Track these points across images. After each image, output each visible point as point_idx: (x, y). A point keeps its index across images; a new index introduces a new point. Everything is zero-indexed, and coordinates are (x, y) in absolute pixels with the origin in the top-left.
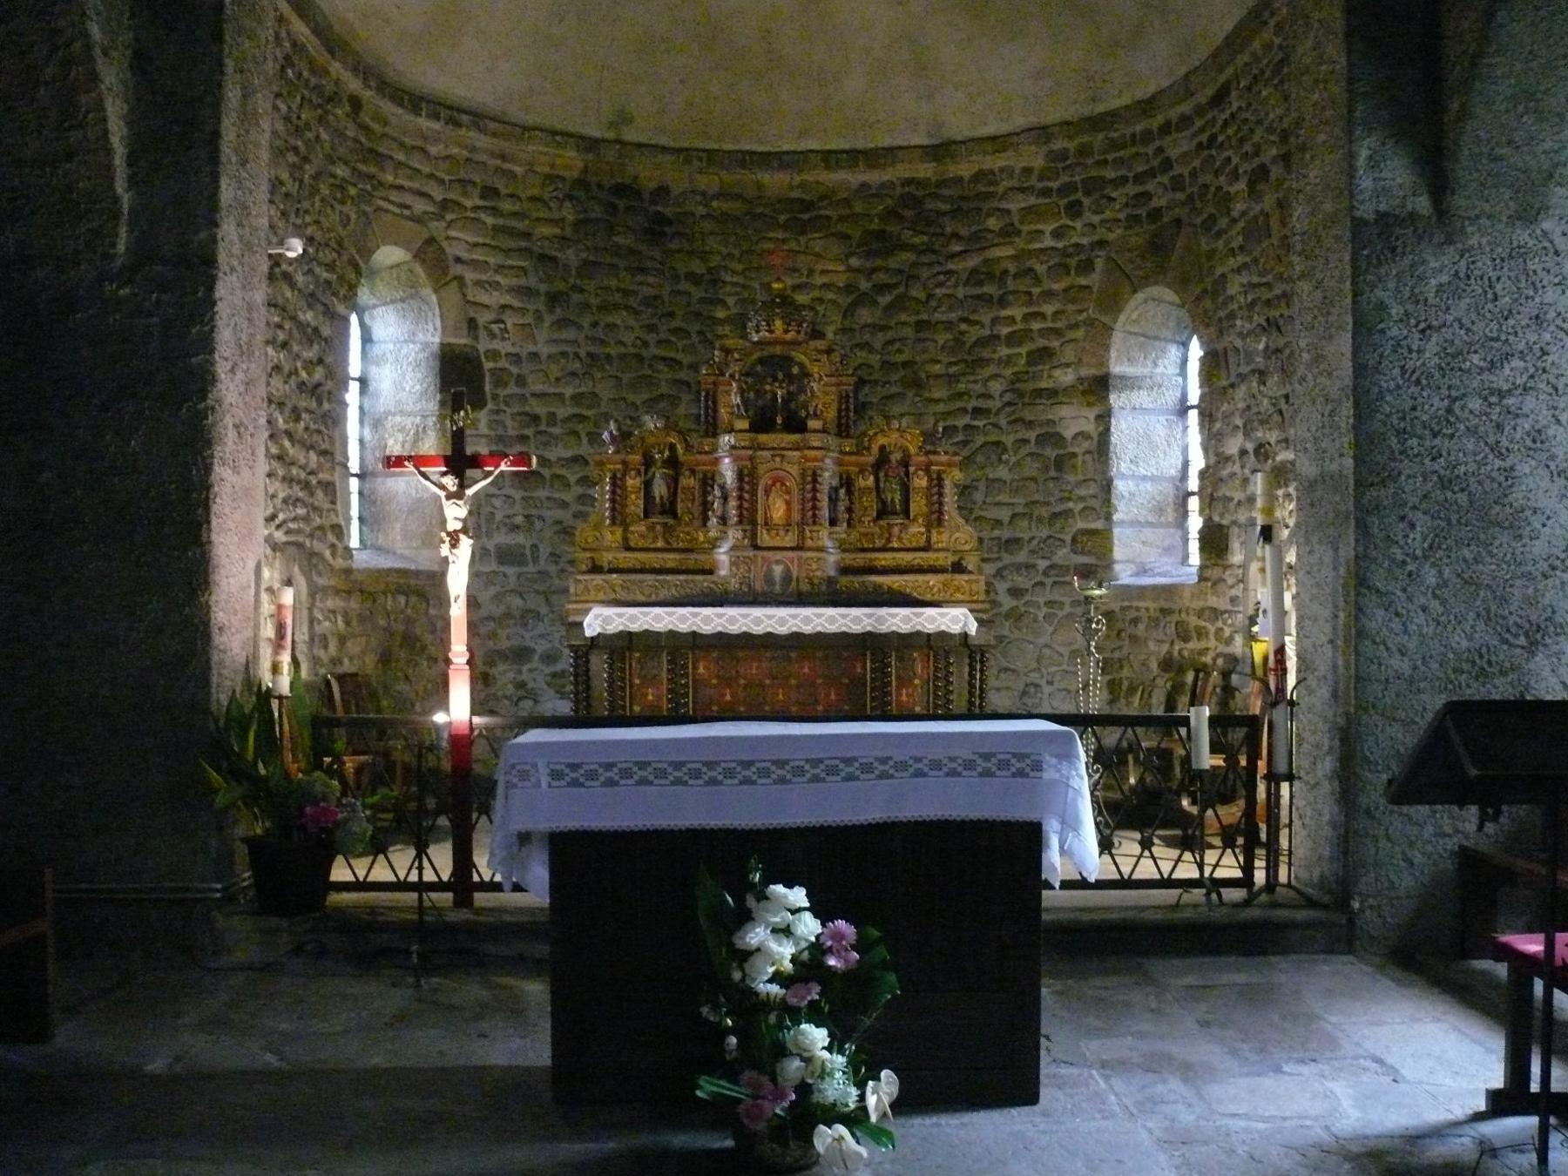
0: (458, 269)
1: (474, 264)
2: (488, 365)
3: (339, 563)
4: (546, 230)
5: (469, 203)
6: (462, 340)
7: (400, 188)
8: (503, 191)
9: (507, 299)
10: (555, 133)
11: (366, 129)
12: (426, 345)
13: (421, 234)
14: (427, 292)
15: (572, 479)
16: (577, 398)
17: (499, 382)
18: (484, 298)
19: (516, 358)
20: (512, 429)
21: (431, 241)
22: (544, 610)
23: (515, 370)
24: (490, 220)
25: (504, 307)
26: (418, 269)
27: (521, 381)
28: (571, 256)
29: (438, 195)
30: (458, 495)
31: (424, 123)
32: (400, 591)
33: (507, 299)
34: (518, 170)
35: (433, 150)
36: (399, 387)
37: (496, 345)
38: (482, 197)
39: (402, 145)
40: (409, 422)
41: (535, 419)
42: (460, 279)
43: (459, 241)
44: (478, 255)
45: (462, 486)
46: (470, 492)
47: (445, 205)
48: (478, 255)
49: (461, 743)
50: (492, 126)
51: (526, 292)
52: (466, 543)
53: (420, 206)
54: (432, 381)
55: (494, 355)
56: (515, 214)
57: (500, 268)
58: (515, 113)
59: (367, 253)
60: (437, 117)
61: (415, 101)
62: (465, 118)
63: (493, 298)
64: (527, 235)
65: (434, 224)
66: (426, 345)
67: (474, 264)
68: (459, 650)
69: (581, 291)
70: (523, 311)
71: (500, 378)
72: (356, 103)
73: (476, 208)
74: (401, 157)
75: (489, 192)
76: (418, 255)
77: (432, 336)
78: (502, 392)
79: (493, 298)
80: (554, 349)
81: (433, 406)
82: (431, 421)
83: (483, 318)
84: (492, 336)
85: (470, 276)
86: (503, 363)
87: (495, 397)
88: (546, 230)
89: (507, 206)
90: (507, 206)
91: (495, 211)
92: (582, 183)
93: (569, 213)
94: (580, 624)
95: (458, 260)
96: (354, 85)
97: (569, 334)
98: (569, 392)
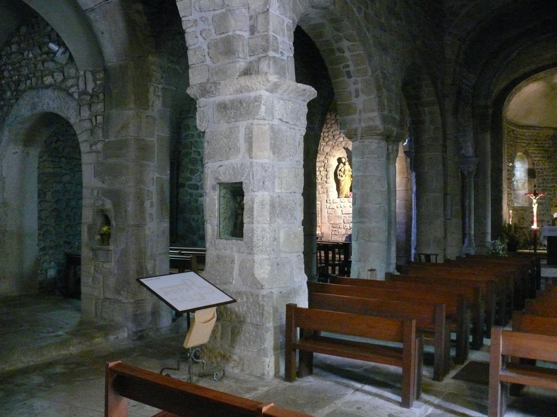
0: (531, 154)
1: (534, 153)
2: (536, 171)
3: (512, 206)
4: (547, 145)
5: (532, 143)
6: (532, 167)
7: (521, 142)
8: (539, 139)
9: (540, 159)
10: (547, 128)
11: (515, 134)
12: (525, 168)
13: (524, 149)
14: (526, 159)
15: (552, 190)
16: (553, 175)
17: (538, 173)
18: (536, 159)
19: (541, 169)
20: (541, 181)
21: (526, 150)
22: (547, 213)
23: (541, 171)
24: (536, 145)
25: (539, 160)
26: (524, 155)
27: (543, 173)
28: (552, 149)
29: (527, 142)
30: (535, 199)
31: (525, 130)
32: (523, 210)
33: (540, 159)
34: (541, 135)
35: (526, 135)
36: (520, 175)
37: (538, 167)
38: (535, 141)
39: (521, 135)
40: (522, 181)
41: (545, 179)
42: (531, 156)
43: (531, 150)
44: (534, 151)
45: (536, 197)
46: (537, 198)
47: (529, 144)
48: (534, 151)
49: (535, 231)
50: (536, 128)
51: (544, 157)
52: (536, 205)
53: (524, 145)
54: (526, 174)
55: (537, 169)
56: (541, 143)
57: (538, 153)
58: (540, 125)
59: (516, 155)
60: (526, 129)
61: (523, 127)
62: (530, 128)
63: (537, 159)
64: (543, 147)
65: (526, 147)
66: (525, 168)
67: (534, 153)
68: (535, 219)
69: (554, 156)
70: (543, 160)
71: (539, 173)
72: (513, 130)
73: (534, 143)
74: (521, 137)
75: (536, 140)
76: (524, 153)
77: (527, 166)
78: (539, 175)
79: (537, 159)
80: (548, 167)
81: (527, 178)
82: (527, 181)
83: (535, 162)
84: (537, 165)
85: (533, 155)
86: (539, 170)
87: (538, 176)
88: (547, 145)
89: (539, 142)
90: (539, 142)
91: (537, 143)
92: (554, 136)
93: (551, 142)
94: (553, 216)
95: (531, 153)
96: (513, 128)
97: (551, 164)
98: (552, 174)
